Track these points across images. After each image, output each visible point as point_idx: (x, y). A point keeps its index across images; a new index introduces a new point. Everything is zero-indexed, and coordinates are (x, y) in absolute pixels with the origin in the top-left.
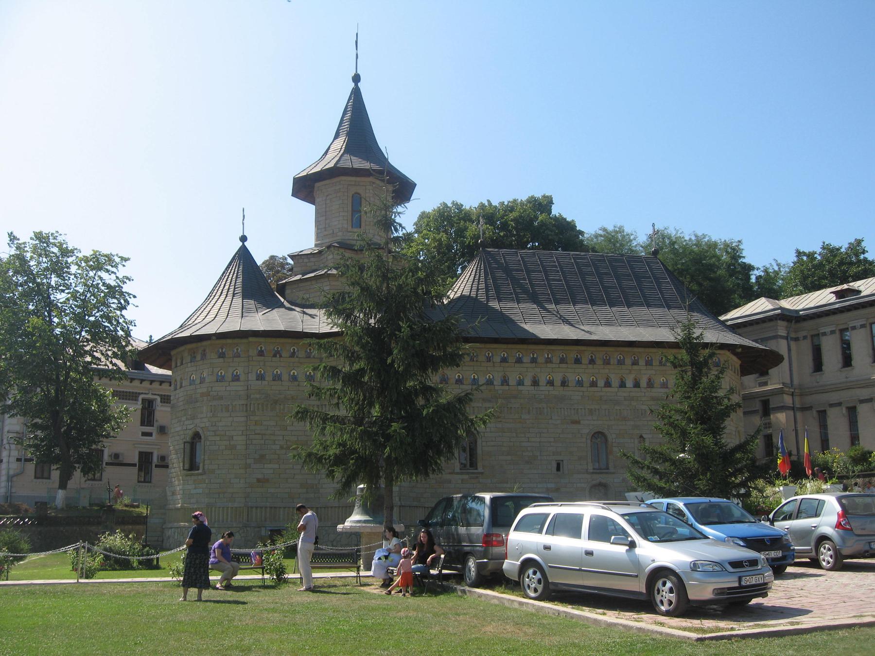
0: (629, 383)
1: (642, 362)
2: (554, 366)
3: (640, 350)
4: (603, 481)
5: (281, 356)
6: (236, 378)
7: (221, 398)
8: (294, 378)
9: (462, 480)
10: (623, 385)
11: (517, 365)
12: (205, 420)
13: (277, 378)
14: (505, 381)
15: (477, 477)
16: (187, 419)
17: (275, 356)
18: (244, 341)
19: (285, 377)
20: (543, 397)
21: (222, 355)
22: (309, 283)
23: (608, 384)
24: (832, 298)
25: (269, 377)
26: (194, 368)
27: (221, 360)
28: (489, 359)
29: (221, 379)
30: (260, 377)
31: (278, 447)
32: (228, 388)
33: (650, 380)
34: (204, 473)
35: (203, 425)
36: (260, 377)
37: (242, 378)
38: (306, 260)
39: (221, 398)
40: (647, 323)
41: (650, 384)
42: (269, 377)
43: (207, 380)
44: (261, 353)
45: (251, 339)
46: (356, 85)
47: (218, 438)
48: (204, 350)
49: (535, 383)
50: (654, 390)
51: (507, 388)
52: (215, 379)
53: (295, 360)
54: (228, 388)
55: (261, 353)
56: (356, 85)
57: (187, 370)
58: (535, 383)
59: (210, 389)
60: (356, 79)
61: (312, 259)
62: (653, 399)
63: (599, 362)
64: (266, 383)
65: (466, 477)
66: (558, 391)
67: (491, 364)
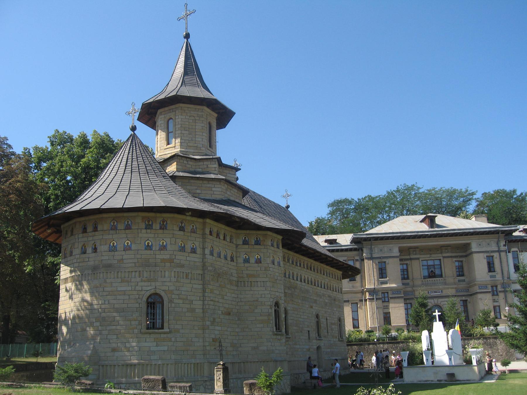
5: (219, 238)
6: (193, 251)
7: (182, 266)
12: (168, 284)
16: (141, 281)
18: (200, 220)
21: (182, 229)
22: (201, 182)
26: (153, 236)
29: (182, 249)
31: (220, 312)
32: (188, 258)
34: (170, 332)
35: (166, 288)
36: (212, 254)
37: (199, 251)
38: (185, 162)
39: (182, 266)
43: (169, 247)
45: (208, 221)
46: (187, 40)
48: (163, 222)
54: (188, 258)
55: (211, 233)
56: (187, 40)
57: (140, 235)
59: (174, 257)
60: (187, 36)
64: (214, 258)
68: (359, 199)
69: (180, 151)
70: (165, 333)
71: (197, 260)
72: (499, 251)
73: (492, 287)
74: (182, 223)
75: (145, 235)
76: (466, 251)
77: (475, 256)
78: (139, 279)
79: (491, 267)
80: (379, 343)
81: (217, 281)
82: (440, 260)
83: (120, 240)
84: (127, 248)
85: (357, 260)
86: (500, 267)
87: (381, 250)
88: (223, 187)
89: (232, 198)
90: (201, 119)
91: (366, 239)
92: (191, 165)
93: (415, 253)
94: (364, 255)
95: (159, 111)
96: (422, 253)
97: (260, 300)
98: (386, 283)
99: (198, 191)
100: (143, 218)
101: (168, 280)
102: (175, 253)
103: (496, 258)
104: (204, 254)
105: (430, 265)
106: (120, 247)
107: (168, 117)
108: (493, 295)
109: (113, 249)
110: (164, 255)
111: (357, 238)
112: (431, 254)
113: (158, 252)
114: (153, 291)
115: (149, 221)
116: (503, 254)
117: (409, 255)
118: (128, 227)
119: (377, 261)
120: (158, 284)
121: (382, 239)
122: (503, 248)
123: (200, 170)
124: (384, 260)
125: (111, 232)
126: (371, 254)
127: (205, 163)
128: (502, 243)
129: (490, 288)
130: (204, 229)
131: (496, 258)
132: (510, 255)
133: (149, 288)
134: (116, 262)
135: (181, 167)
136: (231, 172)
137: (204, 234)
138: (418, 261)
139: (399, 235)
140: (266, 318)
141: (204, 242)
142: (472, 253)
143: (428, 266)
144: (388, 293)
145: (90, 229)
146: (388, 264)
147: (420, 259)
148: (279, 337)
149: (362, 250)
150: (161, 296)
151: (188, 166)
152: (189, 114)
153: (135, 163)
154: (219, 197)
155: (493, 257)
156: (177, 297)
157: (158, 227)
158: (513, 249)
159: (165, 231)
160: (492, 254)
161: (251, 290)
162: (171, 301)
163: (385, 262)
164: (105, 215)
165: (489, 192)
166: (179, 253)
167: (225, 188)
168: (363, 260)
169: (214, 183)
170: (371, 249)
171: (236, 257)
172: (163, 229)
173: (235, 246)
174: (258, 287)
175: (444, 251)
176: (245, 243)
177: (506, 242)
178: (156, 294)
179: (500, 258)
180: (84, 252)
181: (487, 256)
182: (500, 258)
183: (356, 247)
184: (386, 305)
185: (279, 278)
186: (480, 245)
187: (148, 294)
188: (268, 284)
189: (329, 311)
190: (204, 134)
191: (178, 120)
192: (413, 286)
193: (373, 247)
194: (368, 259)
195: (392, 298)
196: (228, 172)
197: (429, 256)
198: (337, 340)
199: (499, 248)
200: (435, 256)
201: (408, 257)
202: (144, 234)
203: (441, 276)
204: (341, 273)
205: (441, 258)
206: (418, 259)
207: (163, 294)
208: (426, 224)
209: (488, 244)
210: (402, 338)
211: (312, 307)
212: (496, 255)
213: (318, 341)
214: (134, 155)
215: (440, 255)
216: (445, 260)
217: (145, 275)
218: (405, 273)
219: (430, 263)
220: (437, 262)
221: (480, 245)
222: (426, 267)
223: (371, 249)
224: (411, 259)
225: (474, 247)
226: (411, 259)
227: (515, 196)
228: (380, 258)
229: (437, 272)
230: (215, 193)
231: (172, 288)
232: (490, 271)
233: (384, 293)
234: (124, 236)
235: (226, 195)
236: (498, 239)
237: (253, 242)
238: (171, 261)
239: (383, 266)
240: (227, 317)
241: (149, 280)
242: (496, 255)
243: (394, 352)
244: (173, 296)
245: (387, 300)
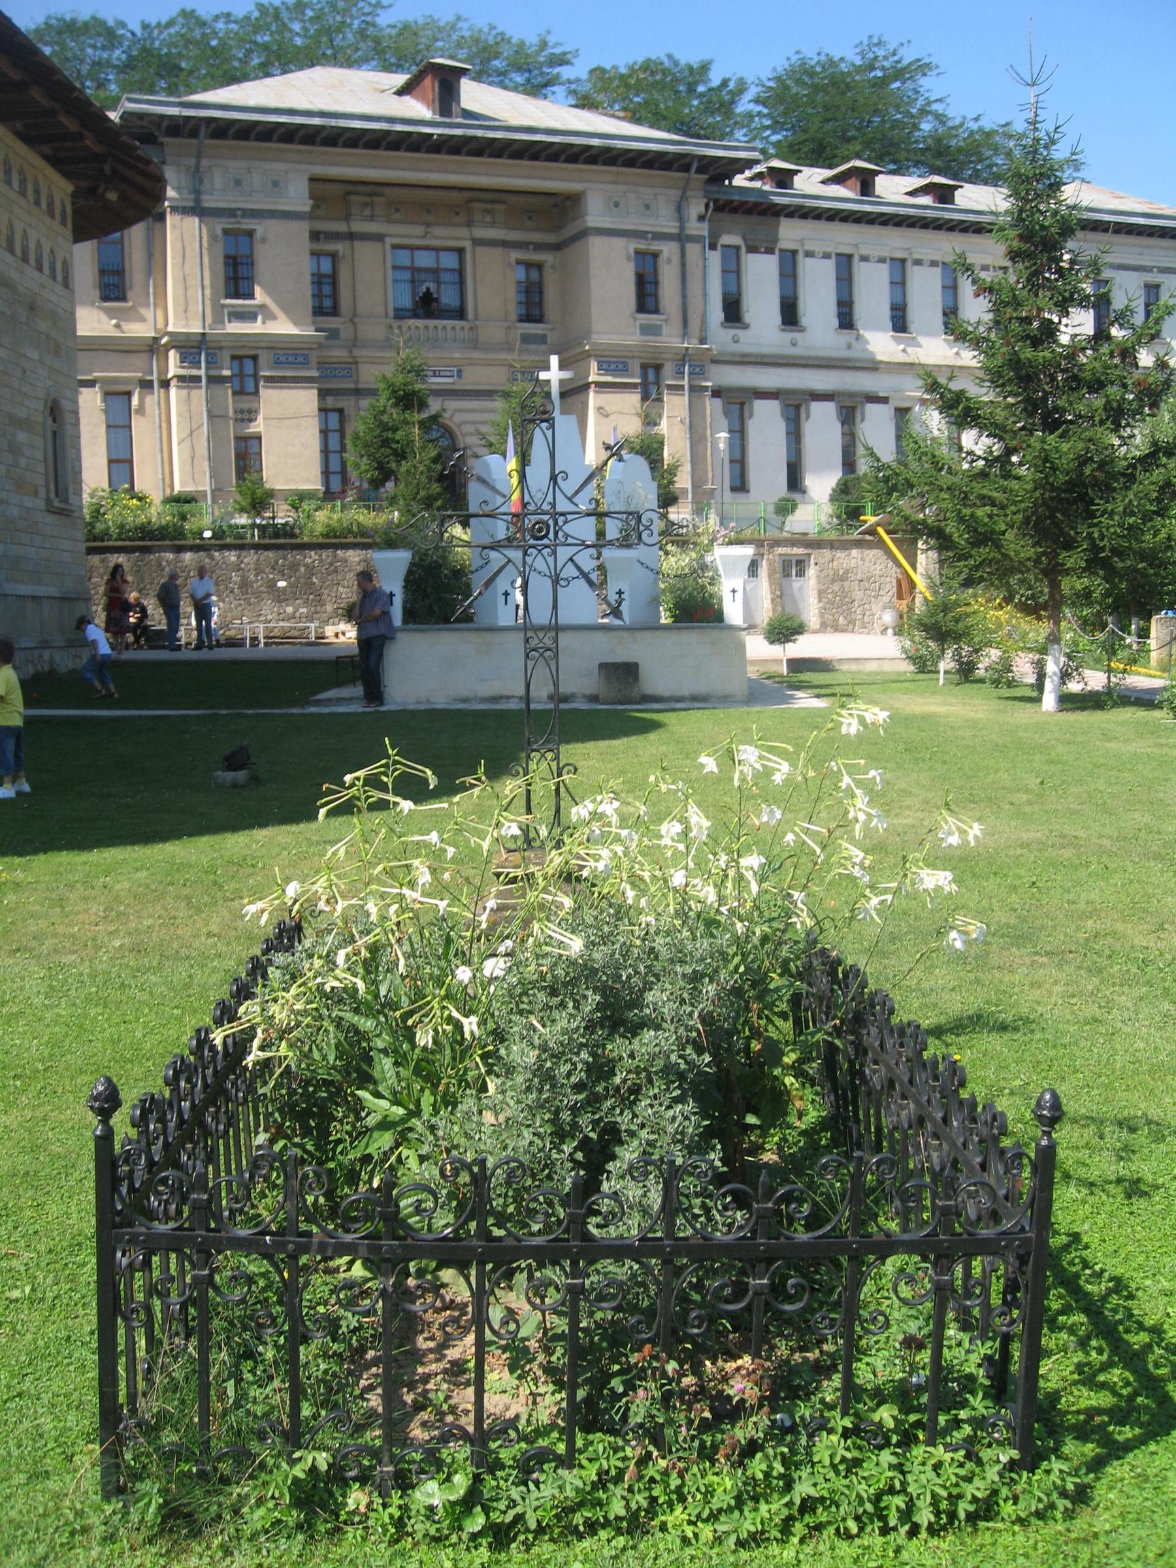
68: (145, 26)
72: (682, 238)
73: (644, 367)
76: (559, 227)
77: (597, 246)
79: (646, 296)
80: (223, 547)
82: (461, 251)
86: (678, 300)
87: (238, 183)
91: (179, 128)
93: (367, 212)
96: (397, 216)
98: (248, 316)
103: (669, 261)
105: (419, 270)
108: (645, 398)
111: (142, 116)
112: (428, 225)
116: (693, 249)
117: (347, 218)
119: (220, 225)
122: (697, 228)
124: (247, 224)
126: (197, 193)
128: (696, 207)
129: (638, 370)
131: (669, 261)
132: (715, 259)
138: (377, 246)
139: (317, 121)
142: (584, 233)
143: (414, 270)
144: (255, 358)
146: (264, 240)
147: (389, 241)
155: (655, 256)
158: (729, 239)
160: (655, 246)
163: (250, 234)
165: (615, 67)
170: (196, 174)
175: (477, 216)
177: (707, 206)
179: (683, 265)
181: (637, 252)
182: (683, 265)
184: (245, 406)
186: (616, 205)
192: (355, 343)
193: (205, 163)
195: (269, 379)
197: (419, 230)
198: (41, 504)
199: (682, 228)
200: (444, 235)
201: (342, 227)
203: (460, 313)
204: (69, 188)
205: (468, 245)
206: (379, 238)
208: (423, 99)
209: (647, 207)
210: (319, 529)
212: (669, 250)
215: (464, 232)
216: (481, 250)
218: (327, 290)
219: (424, 260)
220: (449, 261)
221: (616, 205)
222: (407, 275)
223: (196, 174)
224: (351, 236)
225: (596, 214)
226: (351, 236)
227: (701, 89)
228: (231, 213)
229: (448, 297)
232: (641, 308)
236: (684, 192)
239: (243, 251)
242: (669, 250)
243: (282, 584)
245: (250, 387)
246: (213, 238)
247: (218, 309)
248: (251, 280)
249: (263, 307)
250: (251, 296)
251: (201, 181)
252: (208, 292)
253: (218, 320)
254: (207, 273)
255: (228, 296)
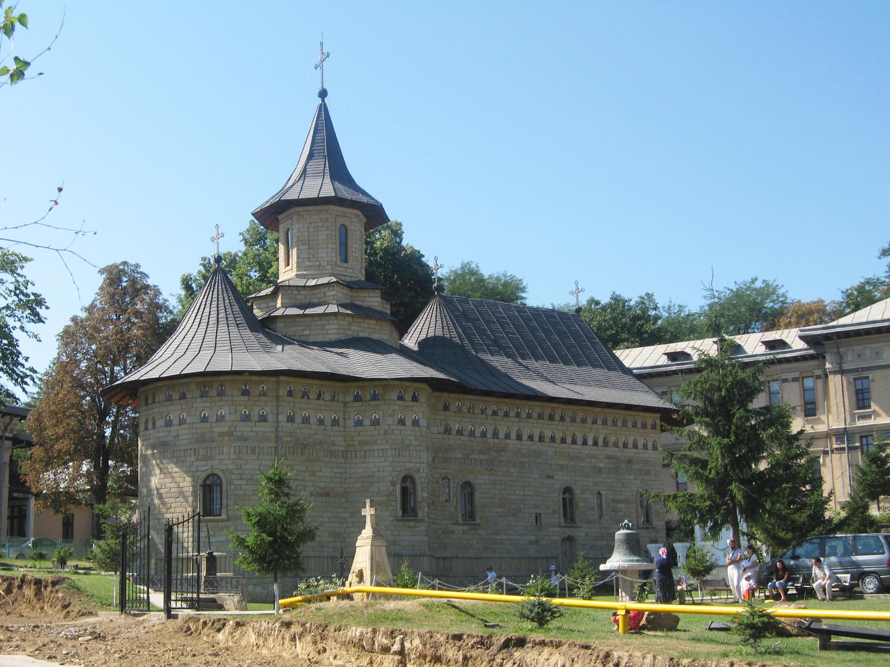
0: (590, 442)
1: (599, 422)
2: (533, 421)
3: (599, 410)
4: (572, 535)
5: (308, 398)
6: (263, 419)
7: (246, 439)
8: (321, 422)
9: (463, 531)
10: (585, 443)
11: (505, 419)
12: (227, 462)
13: (306, 420)
14: (495, 435)
15: (475, 529)
17: (303, 397)
19: (313, 420)
20: (525, 451)
21: (245, 393)
23: (574, 442)
24: (664, 360)
25: (298, 420)
26: (208, 404)
27: (246, 398)
28: (483, 412)
29: (246, 418)
30: (291, 419)
32: (254, 429)
33: (605, 439)
34: (228, 519)
35: (225, 467)
36: (291, 419)
37: (270, 418)
38: (295, 292)
40: (599, 384)
41: (606, 444)
42: (298, 420)
43: (227, 418)
44: (290, 394)
45: (282, 378)
46: (323, 100)
47: (244, 482)
48: (222, 386)
49: (519, 437)
50: (608, 449)
51: (497, 441)
52: (239, 418)
53: (320, 402)
54: (254, 429)
55: (290, 394)
56: (323, 100)
57: (195, 405)
58: (519, 437)
59: (233, 429)
60: (323, 94)
61: (304, 292)
62: (608, 457)
63: (568, 419)
64: (295, 425)
65: (466, 528)
66: (536, 446)
67: (484, 416)
69: (297, 276)
70: (222, 521)
71: (265, 429)
74: (246, 386)
75: (200, 405)
78: (193, 458)
81: (302, 453)
83: (175, 412)
84: (182, 422)
85: (818, 377)
87: (859, 356)
88: (346, 323)
89: (362, 335)
90: (326, 224)
91: (827, 337)
92: (302, 297)
94: (828, 365)
95: (280, 217)
97: (377, 474)
98: (867, 417)
99: (306, 332)
100: (198, 383)
101: (227, 457)
102: (235, 424)
104: (278, 422)
106: (176, 421)
107: (286, 229)
109: (169, 424)
110: (223, 428)
113: (214, 425)
114: (209, 472)
115: (205, 387)
118: (183, 397)
119: (852, 377)
120: (215, 463)
121: (858, 333)
123: (316, 300)
125: (167, 403)
127: (323, 290)
130: (277, 390)
133: (205, 468)
134: (171, 439)
135: (288, 301)
136: (371, 294)
137: (278, 396)
140: (385, 498)
141: (278, 407)
145: (150, 402)
146: (873, 381)
148: (412, 524)
149: (824, 357)
150: (219, 477)
151: (298, 297)
152: (308, 221)
153: (207, 310)
154: (334, 338)
156: (238, 477)
157: (214, 393)
159: (224, 398)
161: (365, 462)
162: (230, 483)
163: (867, 378)
164: (160, 384)
166: (241, 424)
167: (346, 323)
168: (827, 376)
169: (327, 318)
171: (344, 419)
172: (221, 396)
173: (341, 405)
174: (374, 456)
176: (357, 399)
178: (213, 475)
180: (146, 429)
183: (812, 352)
185: (413, 442)
187: (204, 475)
188: (389, 452)
189: (610, 480)
190: (330, 246)
191: (295, 231)
193: (841, 350)
194: (835, 373)
196: (366, 294)
202: (199, 404)
204: (658, 415)
207: (220, 474)
211: (551, 477)
213: (566, 530)
214: (209, 299)
217: (201, 454)
228: (857, 370)
230: (329, 332)
231: (231, 467)
233: (866, 437)
234: (179, 407)
235: (349, 332)
237: (368, 397)
238: (230, 434)
239: (865, 386)
240: (323, 499)
241: (205, 459)
244: (233, 477)
246: (849, 383)
247: (853, 416)
248: (869, 399)
249: (874, 411)
250: (870, 407)
251: (841, 358)
252: (847, 408)
253: (853, 420)
254: (846, 400)
255: (859, 408)
